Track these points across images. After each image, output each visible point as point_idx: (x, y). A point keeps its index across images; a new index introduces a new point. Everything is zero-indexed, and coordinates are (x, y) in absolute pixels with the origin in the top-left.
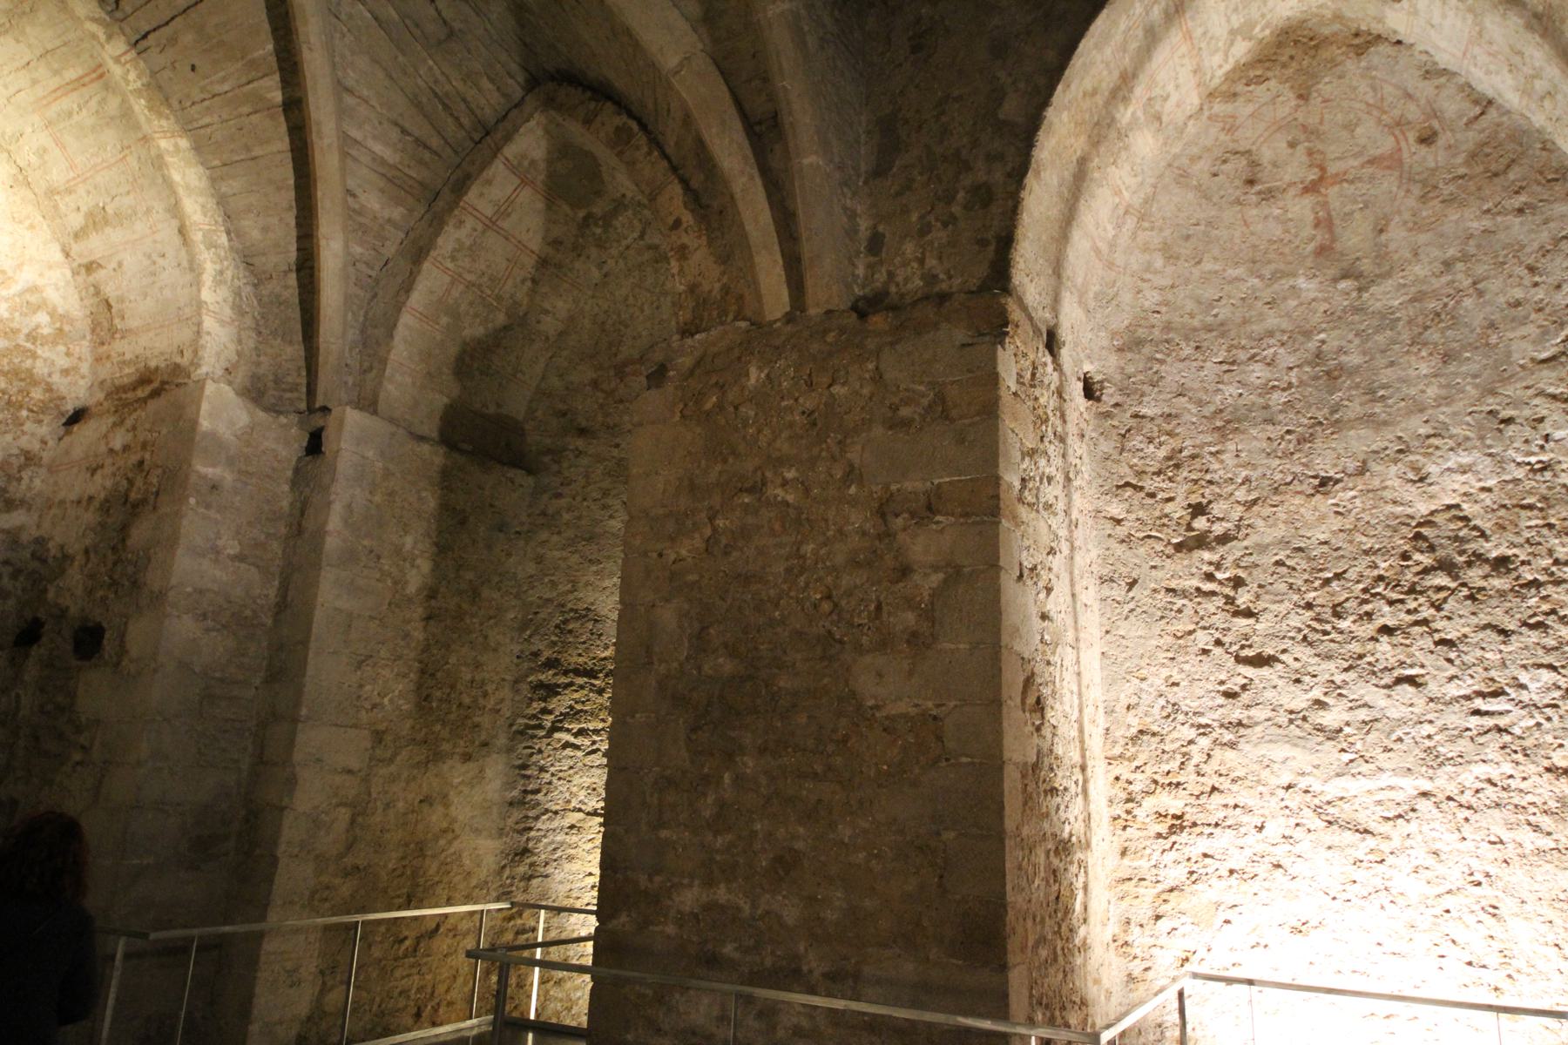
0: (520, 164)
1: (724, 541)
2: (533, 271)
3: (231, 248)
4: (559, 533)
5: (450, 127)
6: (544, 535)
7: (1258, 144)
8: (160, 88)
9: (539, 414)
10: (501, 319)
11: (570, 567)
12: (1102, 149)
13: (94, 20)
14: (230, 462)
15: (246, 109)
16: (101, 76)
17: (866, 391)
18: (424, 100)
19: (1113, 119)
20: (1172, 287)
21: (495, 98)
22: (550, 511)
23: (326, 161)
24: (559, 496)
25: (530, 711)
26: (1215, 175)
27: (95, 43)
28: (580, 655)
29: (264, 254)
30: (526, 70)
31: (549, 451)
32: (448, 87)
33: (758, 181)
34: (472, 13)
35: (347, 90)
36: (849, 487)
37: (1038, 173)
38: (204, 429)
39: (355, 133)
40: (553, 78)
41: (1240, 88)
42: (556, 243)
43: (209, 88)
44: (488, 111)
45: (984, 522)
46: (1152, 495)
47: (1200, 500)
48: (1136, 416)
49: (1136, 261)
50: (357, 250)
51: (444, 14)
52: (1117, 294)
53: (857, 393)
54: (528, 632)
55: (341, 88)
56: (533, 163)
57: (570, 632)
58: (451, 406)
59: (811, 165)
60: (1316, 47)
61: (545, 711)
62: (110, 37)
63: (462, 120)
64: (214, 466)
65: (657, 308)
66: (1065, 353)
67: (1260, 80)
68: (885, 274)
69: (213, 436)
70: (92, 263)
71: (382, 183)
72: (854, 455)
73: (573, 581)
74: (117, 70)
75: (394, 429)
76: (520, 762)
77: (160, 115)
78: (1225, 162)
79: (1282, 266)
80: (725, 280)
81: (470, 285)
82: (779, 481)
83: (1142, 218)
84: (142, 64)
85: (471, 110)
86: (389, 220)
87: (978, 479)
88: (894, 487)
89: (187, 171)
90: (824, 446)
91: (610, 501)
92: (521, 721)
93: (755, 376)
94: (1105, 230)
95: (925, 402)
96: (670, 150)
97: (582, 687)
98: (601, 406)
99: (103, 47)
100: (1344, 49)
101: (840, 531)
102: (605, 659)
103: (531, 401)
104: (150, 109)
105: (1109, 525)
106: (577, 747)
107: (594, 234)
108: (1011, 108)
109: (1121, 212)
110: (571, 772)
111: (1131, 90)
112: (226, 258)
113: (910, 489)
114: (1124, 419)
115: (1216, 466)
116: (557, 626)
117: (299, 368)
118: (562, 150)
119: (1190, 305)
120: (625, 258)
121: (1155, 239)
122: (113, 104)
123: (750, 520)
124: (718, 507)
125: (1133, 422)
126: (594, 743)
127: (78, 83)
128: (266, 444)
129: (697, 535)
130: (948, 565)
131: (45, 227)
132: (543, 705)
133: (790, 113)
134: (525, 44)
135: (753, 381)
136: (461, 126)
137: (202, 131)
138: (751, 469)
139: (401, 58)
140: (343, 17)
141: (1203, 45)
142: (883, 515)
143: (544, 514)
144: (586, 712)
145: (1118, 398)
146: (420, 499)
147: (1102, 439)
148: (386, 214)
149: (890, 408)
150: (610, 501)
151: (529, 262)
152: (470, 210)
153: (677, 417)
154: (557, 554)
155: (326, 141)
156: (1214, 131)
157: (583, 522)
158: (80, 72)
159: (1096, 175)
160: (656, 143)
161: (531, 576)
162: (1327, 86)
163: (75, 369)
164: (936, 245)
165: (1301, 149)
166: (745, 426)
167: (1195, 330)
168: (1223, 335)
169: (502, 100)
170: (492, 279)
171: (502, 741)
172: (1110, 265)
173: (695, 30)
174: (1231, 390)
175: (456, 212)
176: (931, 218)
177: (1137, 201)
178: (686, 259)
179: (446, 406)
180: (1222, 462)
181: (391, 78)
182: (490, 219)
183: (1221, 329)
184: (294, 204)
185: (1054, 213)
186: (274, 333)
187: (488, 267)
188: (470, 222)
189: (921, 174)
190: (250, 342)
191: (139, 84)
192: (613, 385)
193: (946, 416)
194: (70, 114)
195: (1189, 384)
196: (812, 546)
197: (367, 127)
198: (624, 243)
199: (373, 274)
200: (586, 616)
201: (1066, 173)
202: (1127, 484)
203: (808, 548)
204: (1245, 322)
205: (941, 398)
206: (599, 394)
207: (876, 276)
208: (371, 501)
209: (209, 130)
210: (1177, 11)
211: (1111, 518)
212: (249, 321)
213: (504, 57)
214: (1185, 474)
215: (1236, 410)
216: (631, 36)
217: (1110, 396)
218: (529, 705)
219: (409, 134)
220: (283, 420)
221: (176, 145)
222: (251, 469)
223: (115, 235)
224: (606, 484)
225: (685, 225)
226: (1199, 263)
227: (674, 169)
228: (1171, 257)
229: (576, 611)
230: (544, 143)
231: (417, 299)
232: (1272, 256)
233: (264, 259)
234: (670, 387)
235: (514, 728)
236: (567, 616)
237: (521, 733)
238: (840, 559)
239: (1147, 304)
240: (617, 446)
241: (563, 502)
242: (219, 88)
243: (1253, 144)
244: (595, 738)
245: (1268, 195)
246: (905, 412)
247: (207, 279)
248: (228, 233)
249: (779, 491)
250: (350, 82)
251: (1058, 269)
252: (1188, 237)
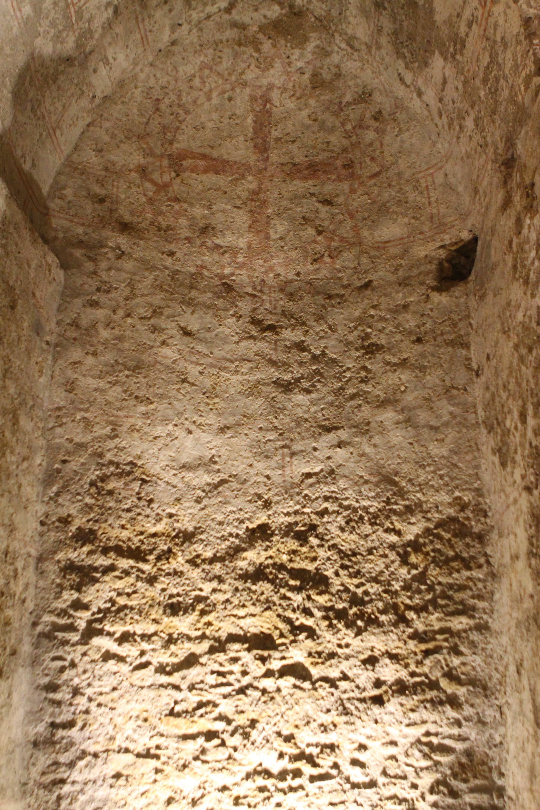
4: (95, 354)
6: (76, 354)
9: (68, 192)
11: (108, 403)
22: (84, 322)
24: (94, 304)
25: (60, 605)
28: (123, 527)
31: (81, 244)
54: (55, 489)
57: (111, 493)
61: (78, 605)
65: (230, 99)
73: (111, 423)
76: (46, 680)
91: (162, 322)
92: (47, 618)
97: (127, 573)
98: (151, 201)
102: (154, 535)
103: (59, 173)
106: (121, 659)
110: (116, 694)
116: (93, 484)
120: (201, 30)
126: (143, 653)
132: (76, 595)
143: (75, 324)
144: (132, 608)
150: (162, 322)
154: (93, 383)
157: (126, 345)
161: (59, 409)
171: (26, 648)
192: (166, 178)
198: (210, 9)
200: (129, 473)
206: (148, 185)
218: (58, 596)
224: (158, 299)
229: (117, 465)
235: (39, 629)
236: (105, 470)
237: (48, 636)
240: (171, 254)
241: (100, 314)
244: (145, 646)
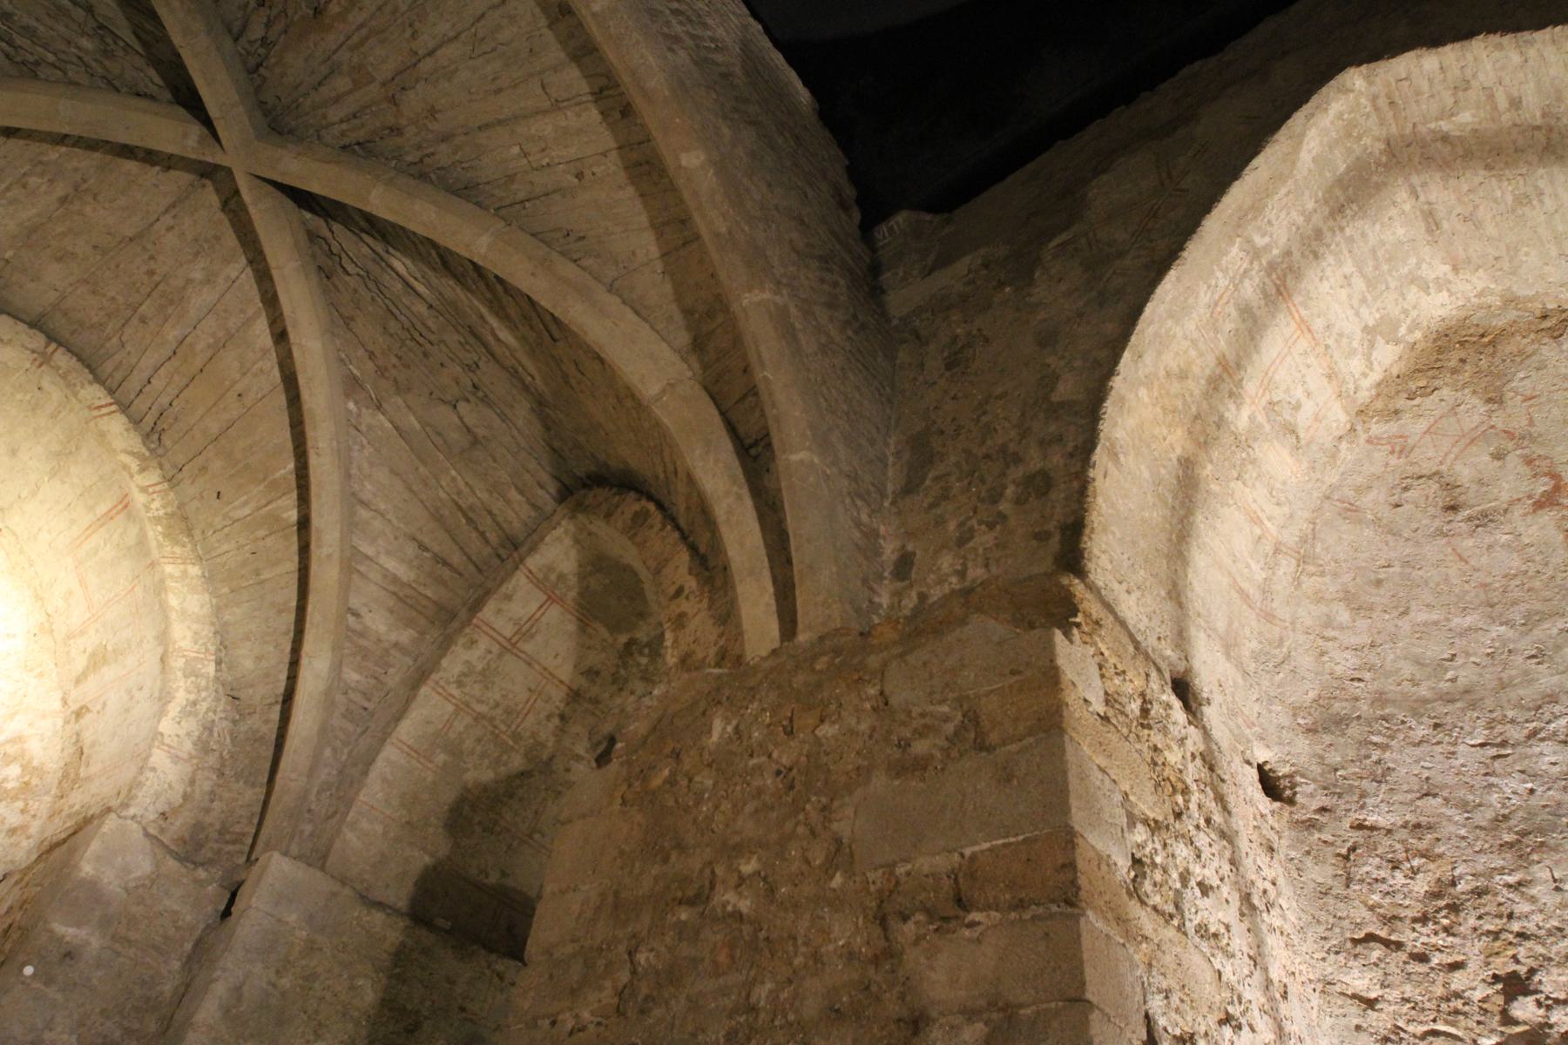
0: (546, 578)
1: (644, 990)
2: (562, 706)
3: (217, 679)
5: (475, 545)
7: (1448, 461)
8: (185, 519)
10: (517, 762)
12: (1215, 455)
13: (132, 454)
14: (106, 922)
15: (261, 533)
16: (126, 506)
17: (864, 727)
18: (446, 513)
19: (1222, 417)
20: (1372, 646)
21: (526, 512)
23: (325, 575)
26: (1397, 506)
27: (125, 473)
29: (252, 686)
30: (555, 477)
32: (471, 500)
33: (748, 502)
34: (499, 421)
35: (363, 503)
36: (832, 878)
37: (1114, 455)
38: (83, 875)
39: (369, 550)
40: (585, 486)
41: (1401, 402)
42: (592, 674)
43: (231, 514)
44: (517, 525)
45: (1052, 916)
46: (1422, 958)
47: (1512, 967)
48: (1360, 826)
49: (1308, 614)
50: (352, 676)
51: (466, 420)
52: (1288, 657)
53: (852, 732)
55: (353, 500)
56: (561, 577)
58: (435, 868)
59: (802, 461)
60: (1492, 343)
62: (143, 470)
63: (488, 534)
64: (79, 925)
66: (1211, 714)
67: (1426, 391)
68: (915, 599)
69: (92, 886)
70: (81, 708)
71: (391, 603)
72: (842, 827)
74: (140, 499)
75: (337, 887)
77: (176, 542)
78: (1406, 489)
79: (1538, 606)
80: (722, 642)
81: (479, 717)
82: (734, 880)
83: (1303, 560)
84: (172, 495)
85: (498, 524)
86: (396, 645)
87: (1035, 840)
88: (901, 870)
89: (189, 597)
90: (801, 817)
93: (719, 729)
94: (1248, 566)
95: (950, 728)
96: (682, 522)
99: (132, 476)
100: (1532, 336)
101: (816, 957)
104: (166, 536)
105: (1354, 1009)
107: (639, 665)
108: (1065, 389)
109: (1269, 549)
111: (1239, 384)
112: (207, 689)
113: (926, 870)
114: (1341, 831)
115: (1523, 907)
117: (253, 814)
118: (596, 563)
119: (1407, 669)
121: (1332, 588)
122: (133, 531)
123: (685, 950)
124: (644, 933)
125: (1357, 836)
127: (108, 517)
128: (167, 902)
129: (608, 984)
130: (992, 1004)
131: (54, 675)
133: (774, 405)
134: (554, 450)
135: (715, 737)
136: (487, 542)
137: (219, 560)
138: (698, 866)
139: (422, 469)
140: (363, 428)
141: (1330, 342)
142: (883, 922)
145: (1322, 800)
146: (352, 988)
147: (1309, 862)
148: (393, 637)
149: (899, 746)
151: (558, 695)
152: (485, 628)
153: (617, 806)
155: (325, 551)
156: (1380, 455)
158: (109, 505)
159: (1214, 487)
160: (671, 518)
162: (1522, 381)
163: (24, 827)
164: (981, 551)
165: (1513, 460)
166: (698, 803)
167: (1425, 701)
168: (1473, 706)
169: (533, 514)
170: (508, 711)
172: (1269, 617)
173: (684, 360)
174: (1513, 785)
175: (467, 630)
176: (974, 522)
177: (1290, 537)
178: (684, 627)
179: (426, 868)
180: (1533, 900)
181: (411, 491)
182: (509, 640)
183: (1469, 697)
184: (292, 627)
185: (1156, 515)
186: (238, 776)
187: (504, 696)
188: (484, 644)
189: (959, 480)
190: (205, 784)
191: (161, 512)
193: (981, 746)
194: (96, 552)
195: (1438, 779)
196: (769, 986)
197: (380, 542)
199: (370, 706)
201: (1163, 471)
202: (1371, 938)
203: (762, 993)
204: (1503, 686)
205: (972, 718)
207: (903, 603)
208: (274, 986)
209: (224, 558)
210: (1279, 293)
211: (1354, 996)
212: (212, 760)
213: (532, 465)
214: (1472, 922)
215: (1531, 814)
216: (633, 396)
217: (1309, 798)
219: (426, 549)
220: (202, 874)
221: (185, 573)
222: (133, 936)
223: (109, 673)
225: (686, 592)
226: (1405, 613)
227: (684, 537)
228: (1360, 608)
230: (573, 553)
231: (407, 729)
232: (1517, 594)
233: (251, 691)
234: (614, 766)
238: (811, 1008)
239: (1339, 670)
242: (240, 513)
243: (1441, 463)
245: (1484, 520)
246: (920, 747)
247: (174, 709)
248: (219, 663)
249: (730, 897)
250: (366, 496)
251: (1176, 594)
252: (1379, 583)
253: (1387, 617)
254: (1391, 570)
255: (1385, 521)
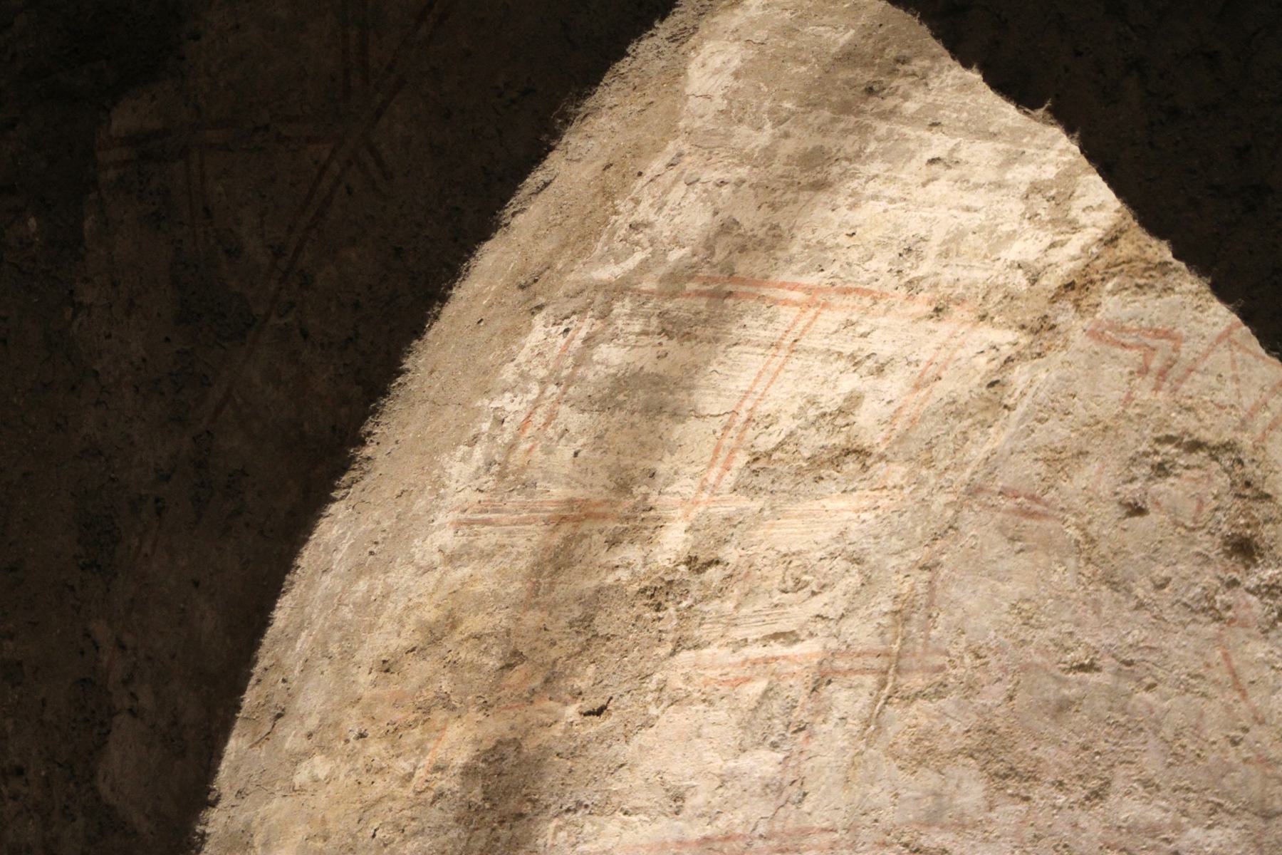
7: (1259, 424)
26: (1136, 510)
78: (1161, 470)
226: (1097, 795)
243: (1243, 426)
253: (1061, 800)
254: (1092, 678)
255: (1103, 548)
